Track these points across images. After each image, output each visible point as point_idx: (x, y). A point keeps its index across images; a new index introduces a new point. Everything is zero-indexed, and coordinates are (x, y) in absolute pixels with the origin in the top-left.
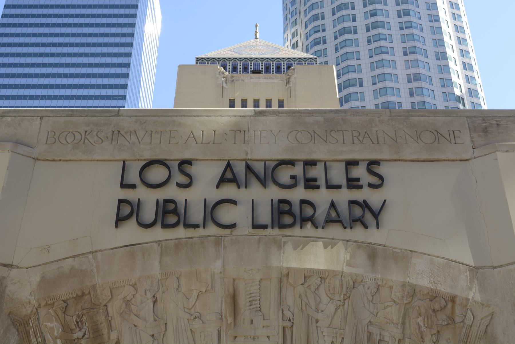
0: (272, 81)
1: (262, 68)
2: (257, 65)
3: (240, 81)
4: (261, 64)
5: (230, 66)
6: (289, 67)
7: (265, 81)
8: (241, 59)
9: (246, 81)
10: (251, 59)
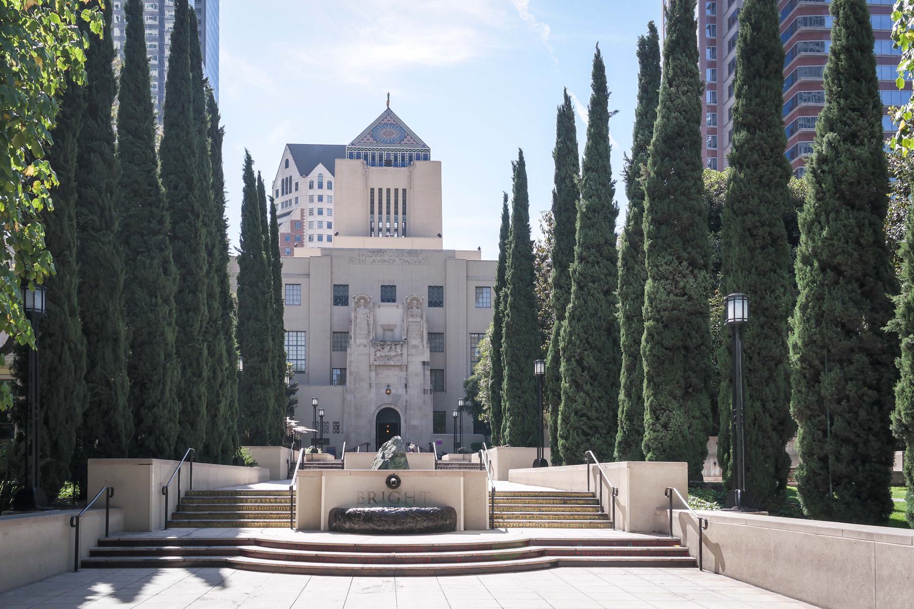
1: (392, 158)
2: (388, 155)
5: (370, 158)
6: (411, 159)
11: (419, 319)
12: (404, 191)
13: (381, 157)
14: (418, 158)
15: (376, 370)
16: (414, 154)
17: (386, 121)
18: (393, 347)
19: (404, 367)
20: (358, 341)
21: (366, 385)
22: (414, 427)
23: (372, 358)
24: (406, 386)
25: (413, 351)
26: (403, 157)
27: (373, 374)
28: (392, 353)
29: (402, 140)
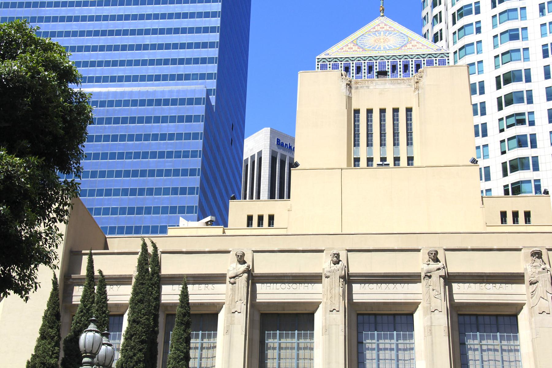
0: (398, 86)
1: (388, 68)
2: (382, 65)
3: (365, 88)
4: (387, 64)
5: (353, 69)
6: (418, 67)
7: (392, 86)
8: (365, 58)
9: (371, 87)
10: (375, 58)
12: (409, 110)
13: (370, 69)
14: (430, 63)
16: (423, 61)
17: (377, 28)
26: (406, 67)
29: (405, 45)
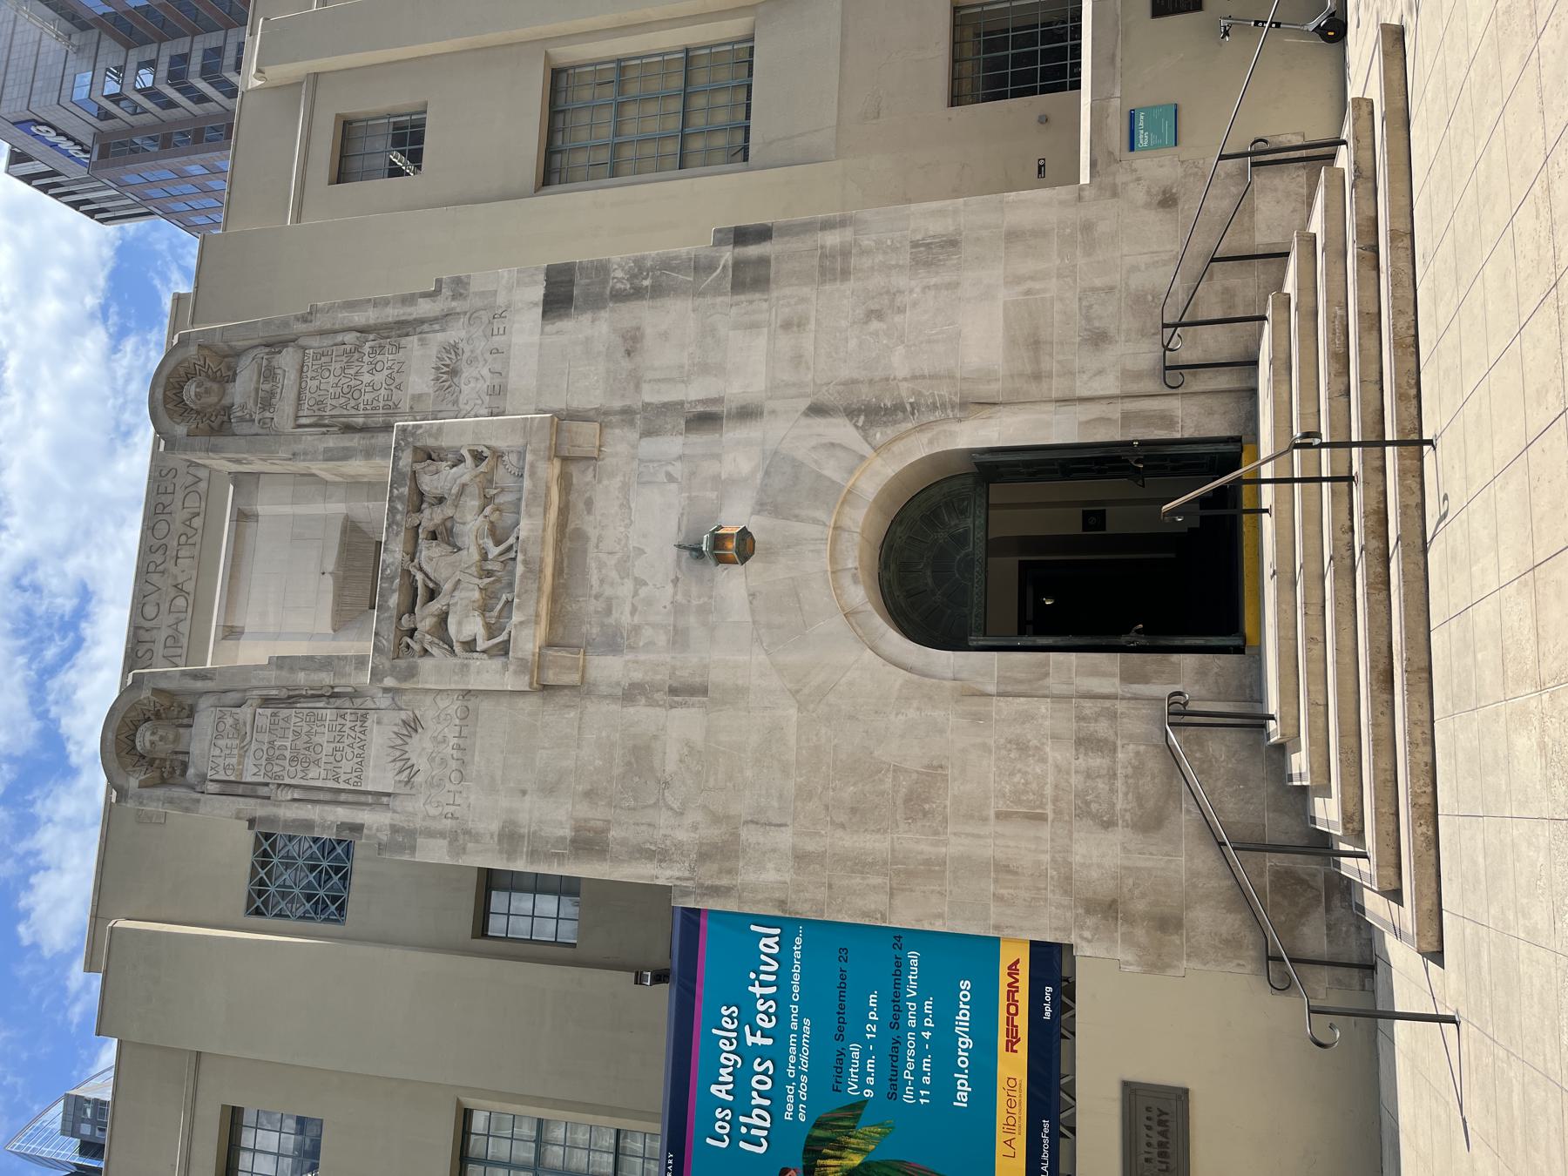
11: (287, 360)
15: (587, 646)
18: (431, 517)
19: (569, 443)
20: (379, 778)
21: (681, 726)
22: (1031, 343)
23: (487, 674)
24: (705, 420)
25: (473, 382)
27: (608, 668)
28: (471, 524)
